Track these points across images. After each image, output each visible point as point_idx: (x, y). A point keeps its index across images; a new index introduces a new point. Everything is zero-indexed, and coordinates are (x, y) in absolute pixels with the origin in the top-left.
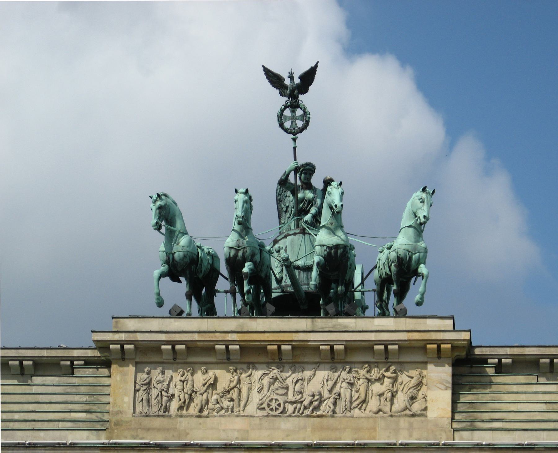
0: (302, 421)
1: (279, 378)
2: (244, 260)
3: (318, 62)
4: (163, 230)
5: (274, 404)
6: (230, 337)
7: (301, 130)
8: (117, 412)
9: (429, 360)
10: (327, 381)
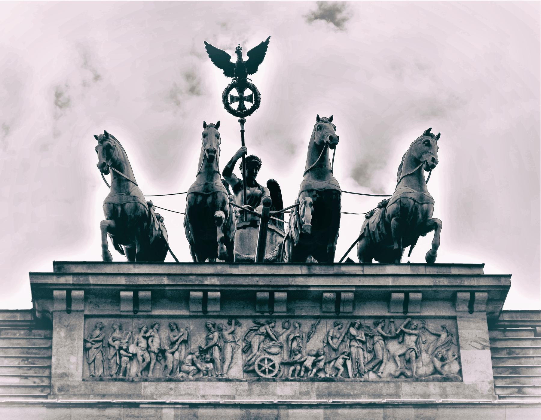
0: (304, 386)
1: (271, 333)
2: (215, 208)
3: (270, 37)
4: (109, 177)
5: (266, 366)
6: (208, 281)
7: (250, 112)
8: (61, 374)
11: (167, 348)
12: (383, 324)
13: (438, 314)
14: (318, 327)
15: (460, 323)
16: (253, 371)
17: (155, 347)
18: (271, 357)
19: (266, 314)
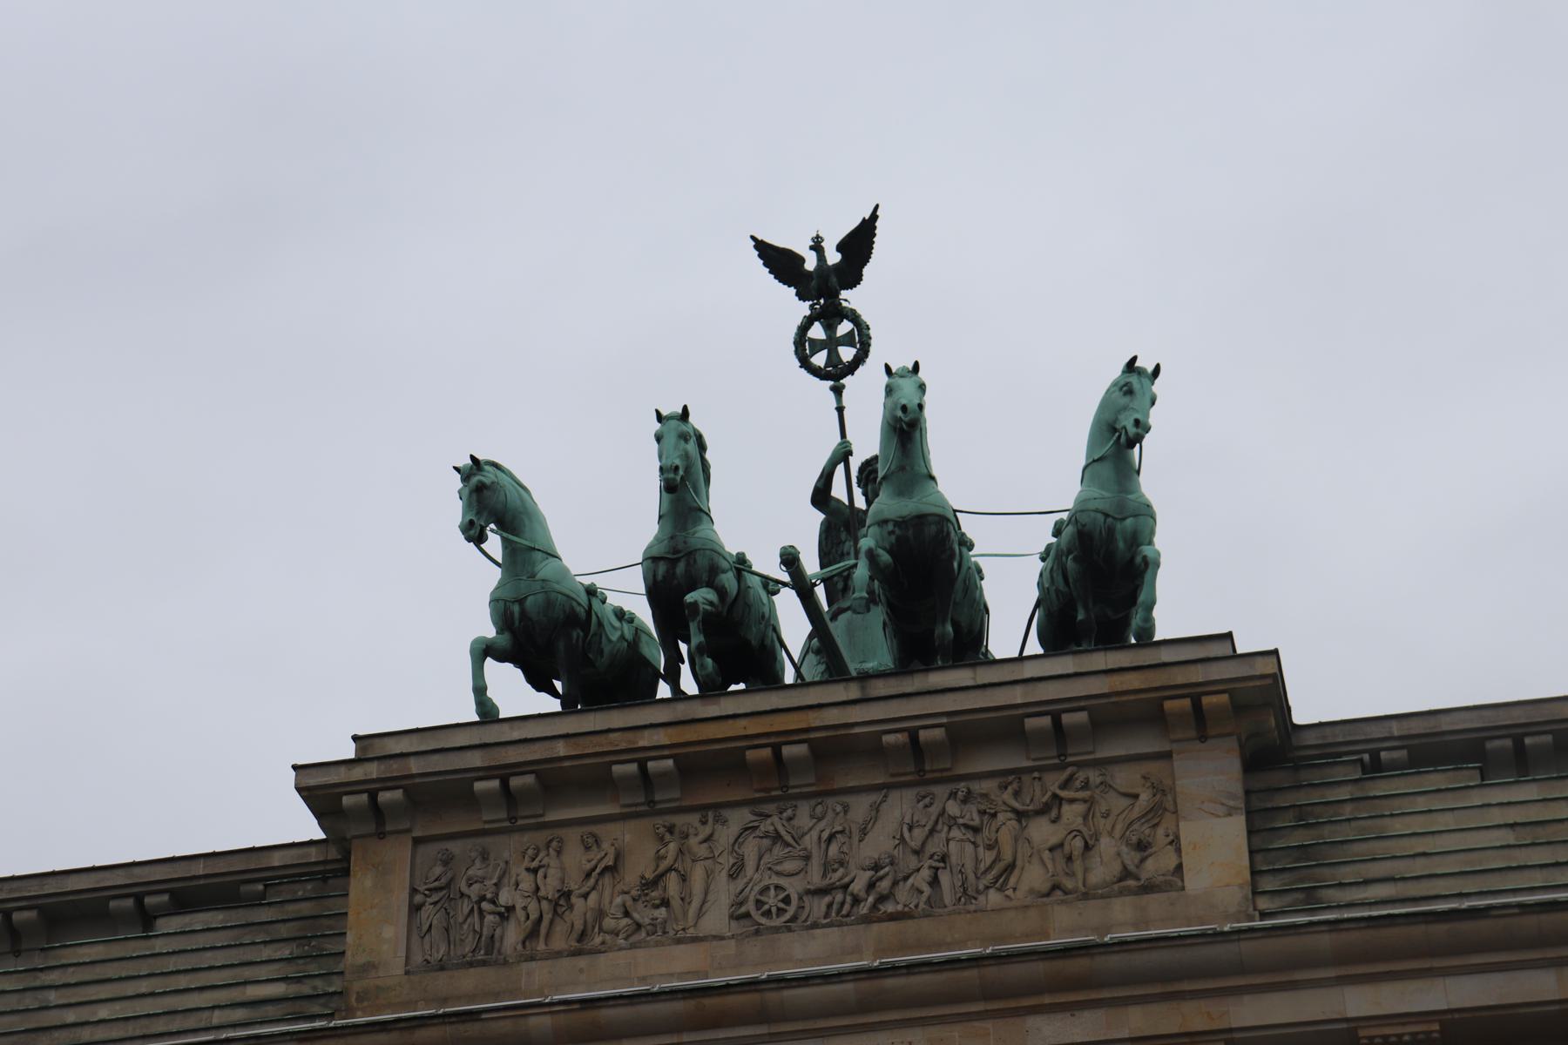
1: (783, 833)
3: (877, 207)
5: (772, 900)
6: (646, 739)
7: (852, 367)
9: (1175, 746)
10: (910, 829)
11: (573, 886)
12: (1015, 785)
13: (1132, 752)
14: (884, 806)
15: (1178, 763)
16: (747, 915)
17: (550, 887)
18: (782, 881)
19: (774, 793)
